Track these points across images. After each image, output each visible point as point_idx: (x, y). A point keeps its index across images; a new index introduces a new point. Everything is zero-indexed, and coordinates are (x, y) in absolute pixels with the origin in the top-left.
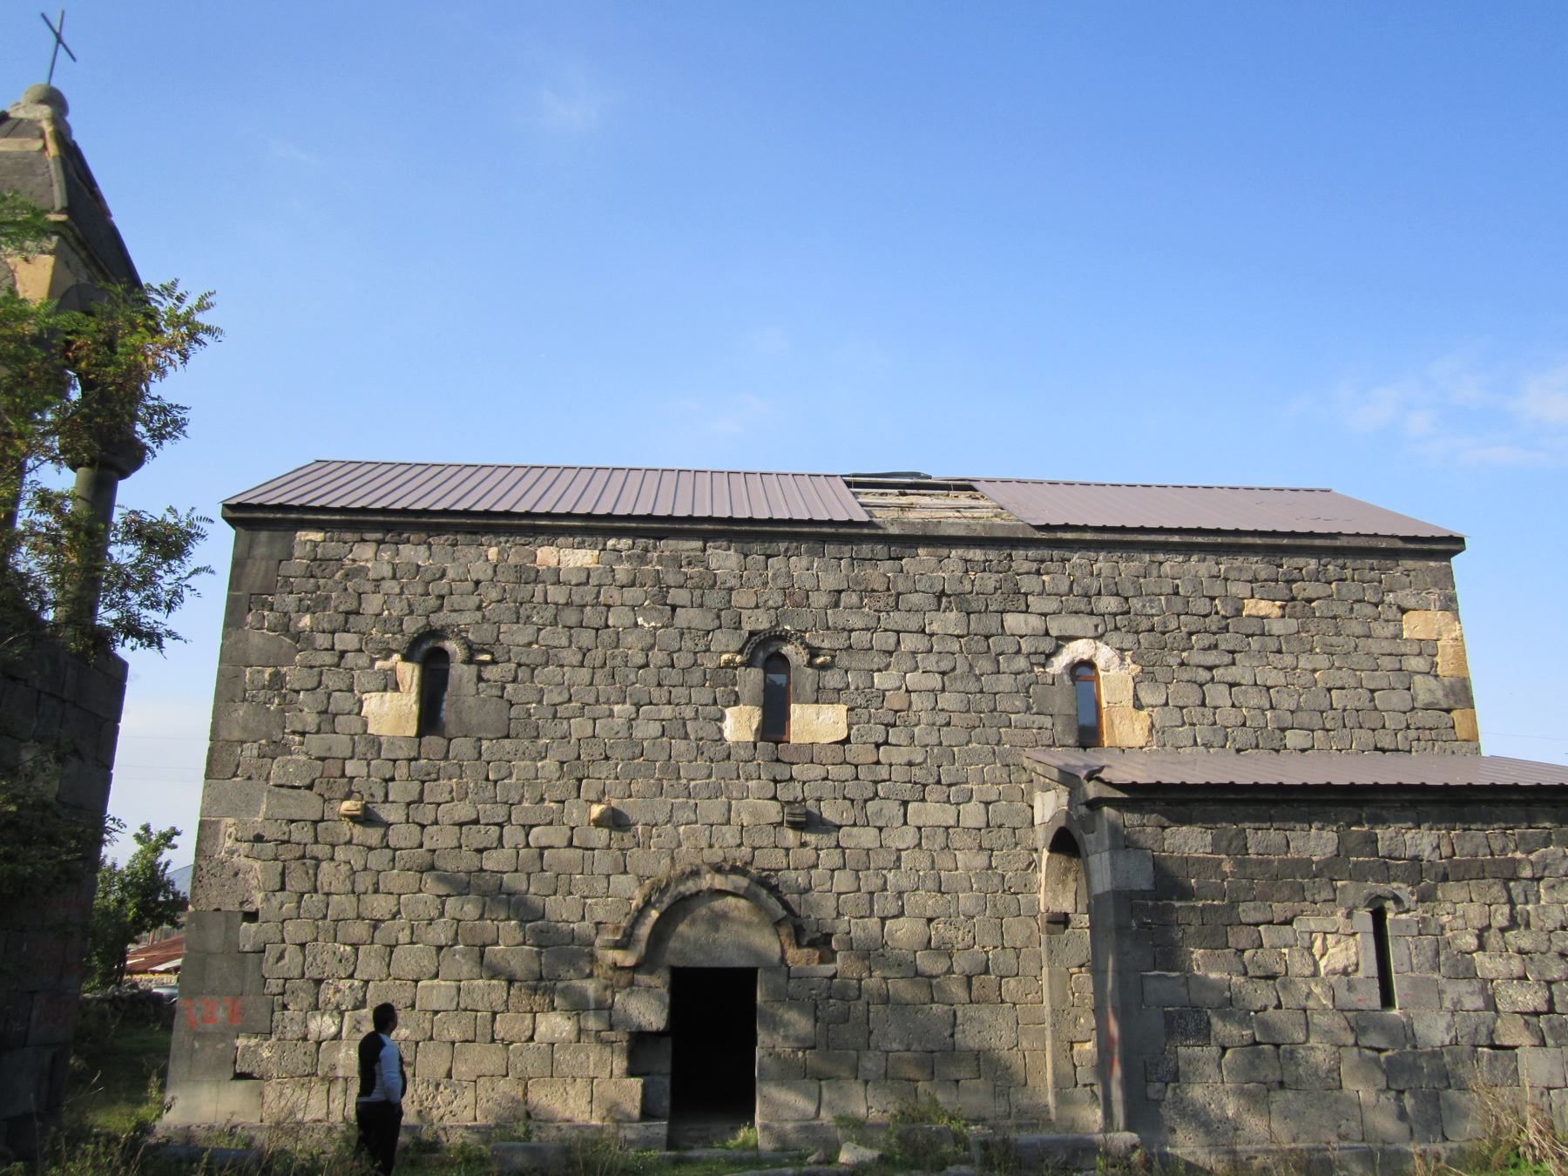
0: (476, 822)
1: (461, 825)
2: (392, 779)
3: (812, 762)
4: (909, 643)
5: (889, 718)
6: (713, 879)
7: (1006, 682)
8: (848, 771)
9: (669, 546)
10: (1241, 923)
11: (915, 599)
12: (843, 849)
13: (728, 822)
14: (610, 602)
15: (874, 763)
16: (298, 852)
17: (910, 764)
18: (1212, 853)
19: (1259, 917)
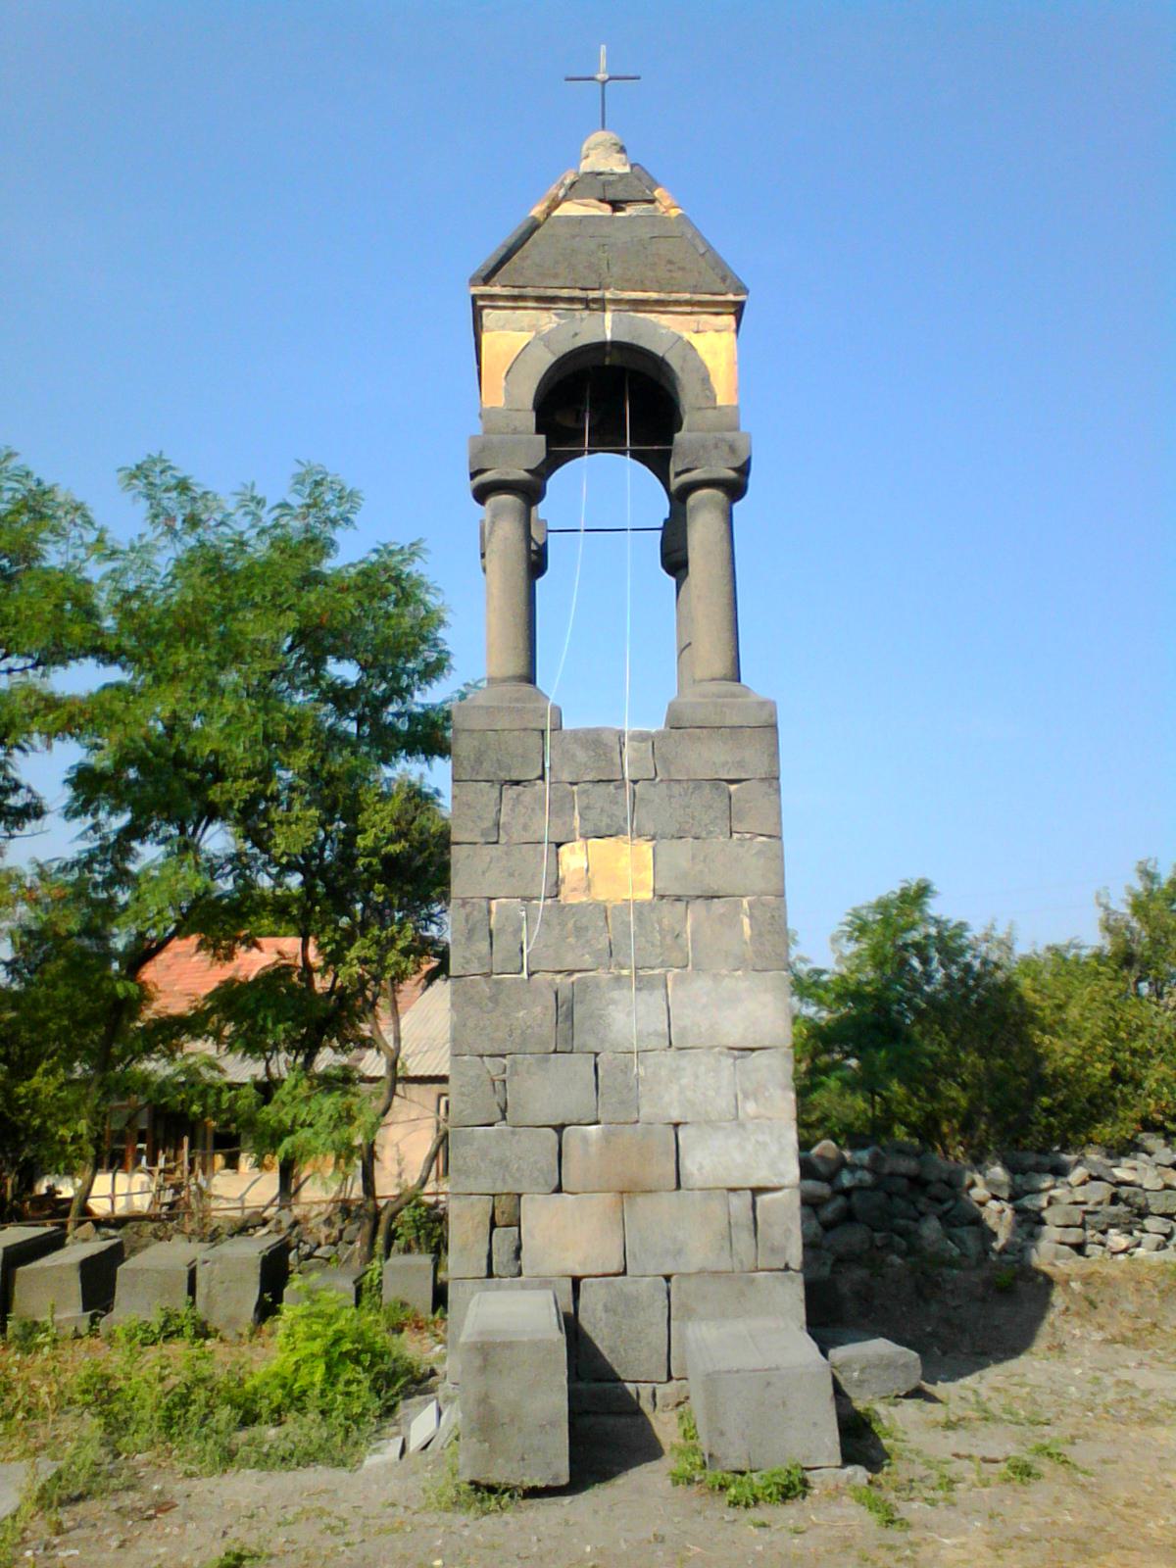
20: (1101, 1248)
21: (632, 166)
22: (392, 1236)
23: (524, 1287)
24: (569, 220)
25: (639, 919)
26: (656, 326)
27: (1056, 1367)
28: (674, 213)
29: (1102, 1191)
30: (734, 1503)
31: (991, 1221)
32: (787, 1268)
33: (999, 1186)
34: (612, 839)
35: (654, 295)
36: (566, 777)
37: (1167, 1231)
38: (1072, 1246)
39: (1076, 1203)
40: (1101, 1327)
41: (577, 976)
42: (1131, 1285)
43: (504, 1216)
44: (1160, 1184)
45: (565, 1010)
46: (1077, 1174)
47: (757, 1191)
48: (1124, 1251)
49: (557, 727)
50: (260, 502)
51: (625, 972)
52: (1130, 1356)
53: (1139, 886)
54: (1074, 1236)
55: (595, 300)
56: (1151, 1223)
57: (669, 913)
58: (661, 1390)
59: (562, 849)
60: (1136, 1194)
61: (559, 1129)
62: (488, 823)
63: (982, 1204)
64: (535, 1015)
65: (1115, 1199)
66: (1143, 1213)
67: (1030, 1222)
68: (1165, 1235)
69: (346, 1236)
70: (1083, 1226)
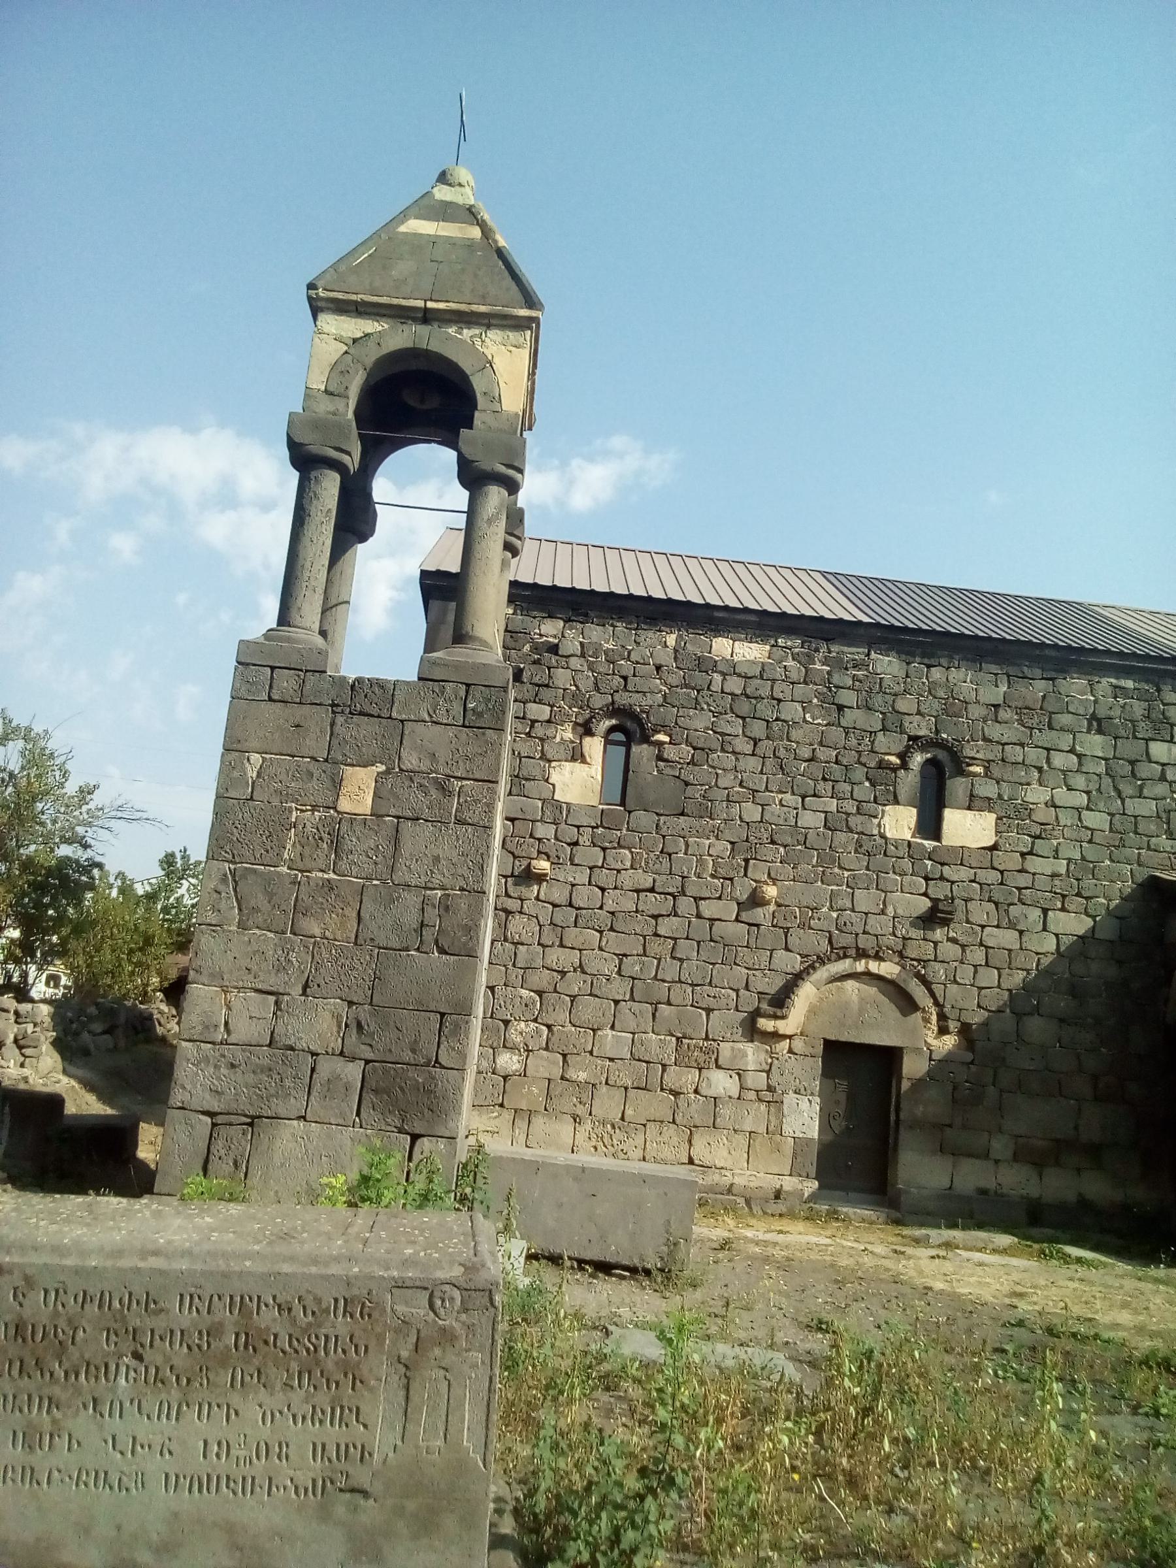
0: (652, 890)
1: (638, 891)
2: (576, 844)
3: (961, 864)
4: (1059, 760)
5: (1036, 830)
6: (867, 963)
7: (1147, 808)
8: (994, 877)
11: (1065, 719)
12: (986, 947)
13: (883, 912)
14: (781, 696)
15: (1019, 871)
17: (1054, 875)
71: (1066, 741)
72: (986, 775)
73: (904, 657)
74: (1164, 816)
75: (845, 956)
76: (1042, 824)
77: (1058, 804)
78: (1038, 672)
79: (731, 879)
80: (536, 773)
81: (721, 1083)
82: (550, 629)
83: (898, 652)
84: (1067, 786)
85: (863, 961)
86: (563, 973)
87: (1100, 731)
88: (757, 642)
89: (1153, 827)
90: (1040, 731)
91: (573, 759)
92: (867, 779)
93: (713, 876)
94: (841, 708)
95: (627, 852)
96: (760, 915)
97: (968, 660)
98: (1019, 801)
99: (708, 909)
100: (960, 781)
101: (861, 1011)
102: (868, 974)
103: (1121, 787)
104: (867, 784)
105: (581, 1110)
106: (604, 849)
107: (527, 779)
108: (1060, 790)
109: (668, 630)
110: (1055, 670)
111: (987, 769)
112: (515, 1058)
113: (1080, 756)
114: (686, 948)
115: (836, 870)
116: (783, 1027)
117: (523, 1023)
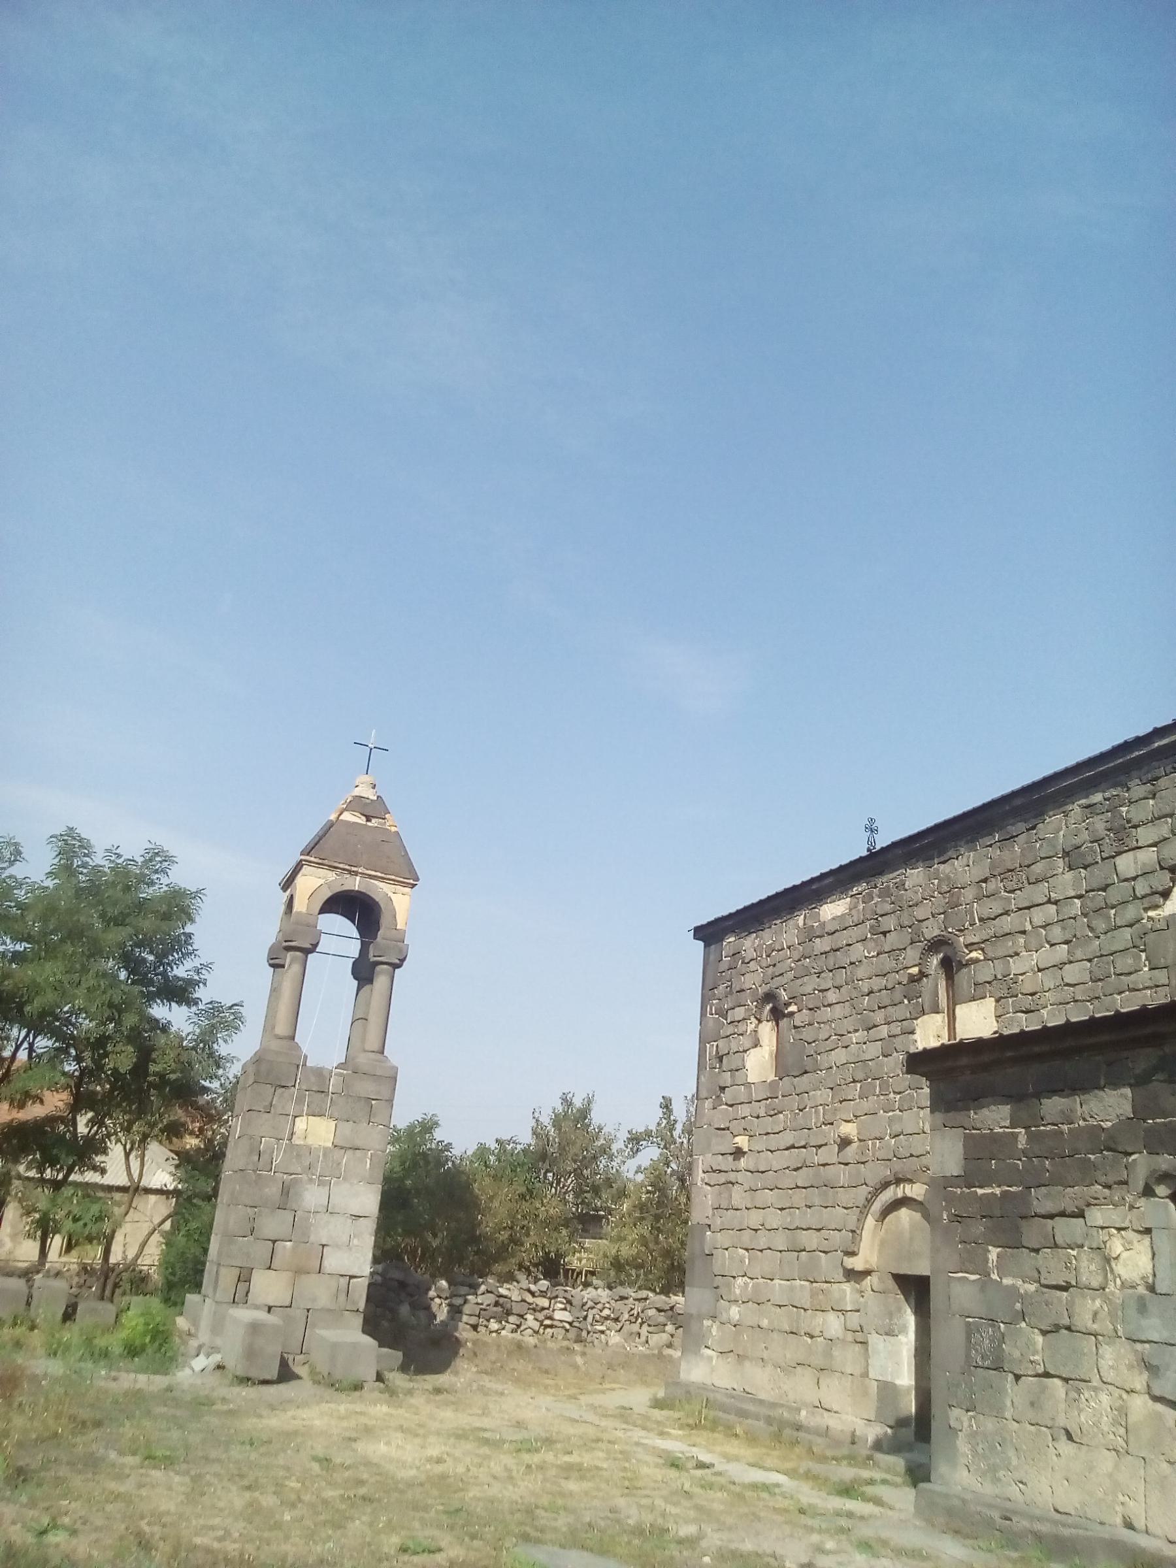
0: (793, 1147)
2: (758, 1117)
9: (887, 880)
10: (1036, 1215)
11: (1038, 868)
16: (722, 1178)
18: (1012, 1126)
19: (1049, 1207)
20: (485, 1328)
21: (378, 797)
22: (116, 1286)
23: (247, 1308)
24: (347, 823)
25: (324, 1155)
26: (377, 886)
27: (453, 1379)
28: (393, 829)
29: (490, 1299)
30: (337, 1390)
31: (434, 1308)
32: (358, 1310)
33: (441, 1290)
34: (319, 1118)
35: (379, 874)
36: (304, 1087)
37: (518, 1323)
38: (472, 1326)
39: (477, 1304)
40: (477, 1366)
41: (293, 1176)
42: (495, 1348)
43: (244, 1277)
44: (519, 1299)
45: (286, 1191)
46: (483, 1288)
47: (351, 1277)
48: (496, 1331)
49: (304, 1065)
50: (119, 856)
51: (314, 1177)
52: (486, 1378)
53: (560, 1109)
54: (473, 1320)
55: (353, 872)
56: (512, 1319)
57: (338, 1153)
58: (298, 1358)
59: (297, 1119)
60: (507, 1303)
61: (274, 1242)
62: (267, 1104)
63: (432, 1299)
64: (272, 1191)
65: (497, 1304)
66: (509, 1313)
67: (456, 1311)
68: (517, 1325)
69: (88, 1284)
70: (479, 1316)
71: (1039, 893)
72: (986, 959)
73: (928, 863)
74: (1138, 942)
75: (885, 1185)
76: (1032, 994)
77: (1041, 966)
78: (1022, 826)
79: (832, 1124)
80: (740, 1065)
81: (833, 1324)
82: (749, 944)
83: (924, 861)
84: (1048, 942)
85: (902, 1185)
86: (756, 1230)
87: (1071, 869)
88: (843, 898)
89: (1130, 961)
90: (1020, 889)
91: (756, 1046)
92: (905, 997)
93: (824, 1123)
94: (884, 933)
95: (781, 1115)
96: (851, 1151)
97: (967, 842)
98: (1012, 976)
99: (823, 1155)
100: (965, 970)
101: (911, 1239)
102: (904, 1202)
103: (1094, 923)
104: (906, 1001)
105: (765, 1355)
106: (771, 1116)
107: (737, 1070)
108: (1044, 949)
109: (798, 913)
110: (1036, 817)
111: (982, 949)
112: (737, 1309)
113: (1056, 903)
114: (815, 1197)
115: (892, 1095)
116: (856, 1263)
117: (741, 1278)
